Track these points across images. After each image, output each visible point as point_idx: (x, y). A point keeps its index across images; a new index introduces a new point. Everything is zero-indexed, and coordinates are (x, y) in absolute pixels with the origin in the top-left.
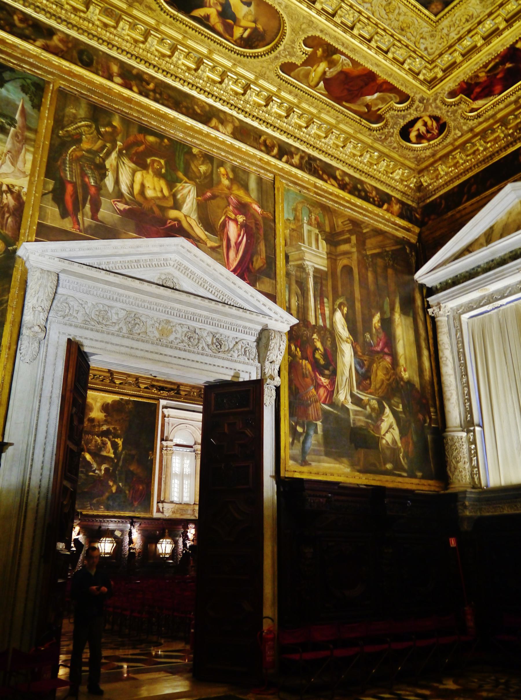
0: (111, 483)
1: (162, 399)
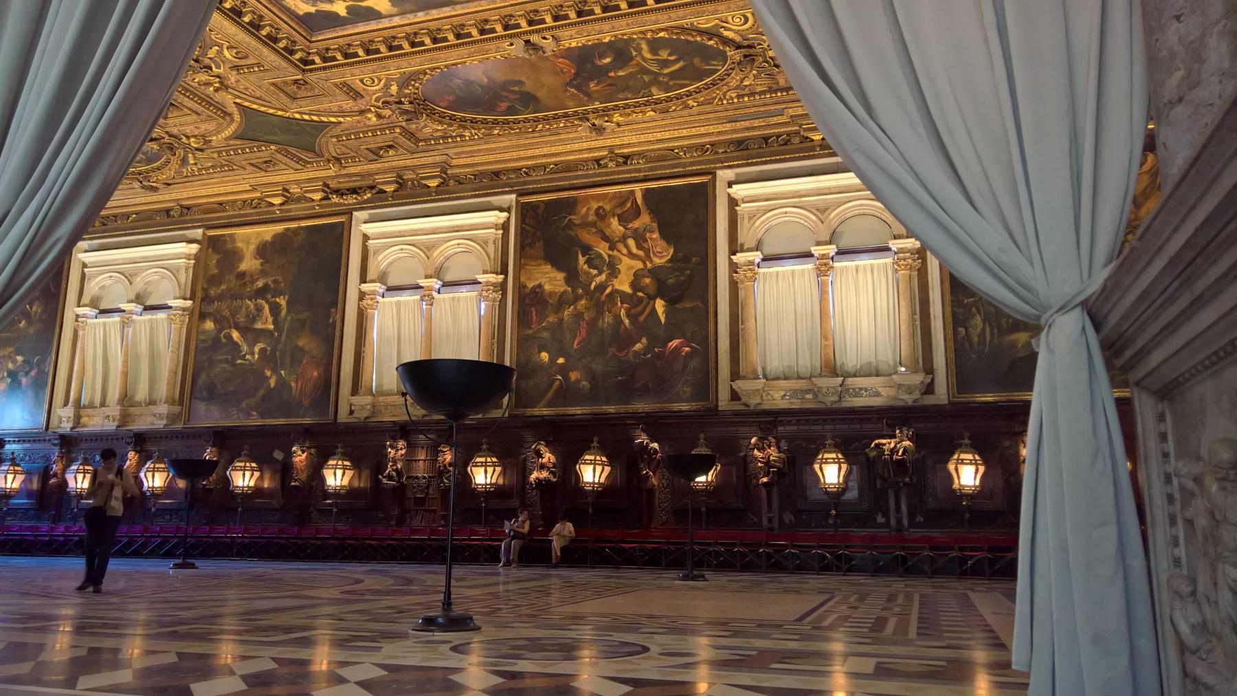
0: (268, 373)
1: (356, 209)
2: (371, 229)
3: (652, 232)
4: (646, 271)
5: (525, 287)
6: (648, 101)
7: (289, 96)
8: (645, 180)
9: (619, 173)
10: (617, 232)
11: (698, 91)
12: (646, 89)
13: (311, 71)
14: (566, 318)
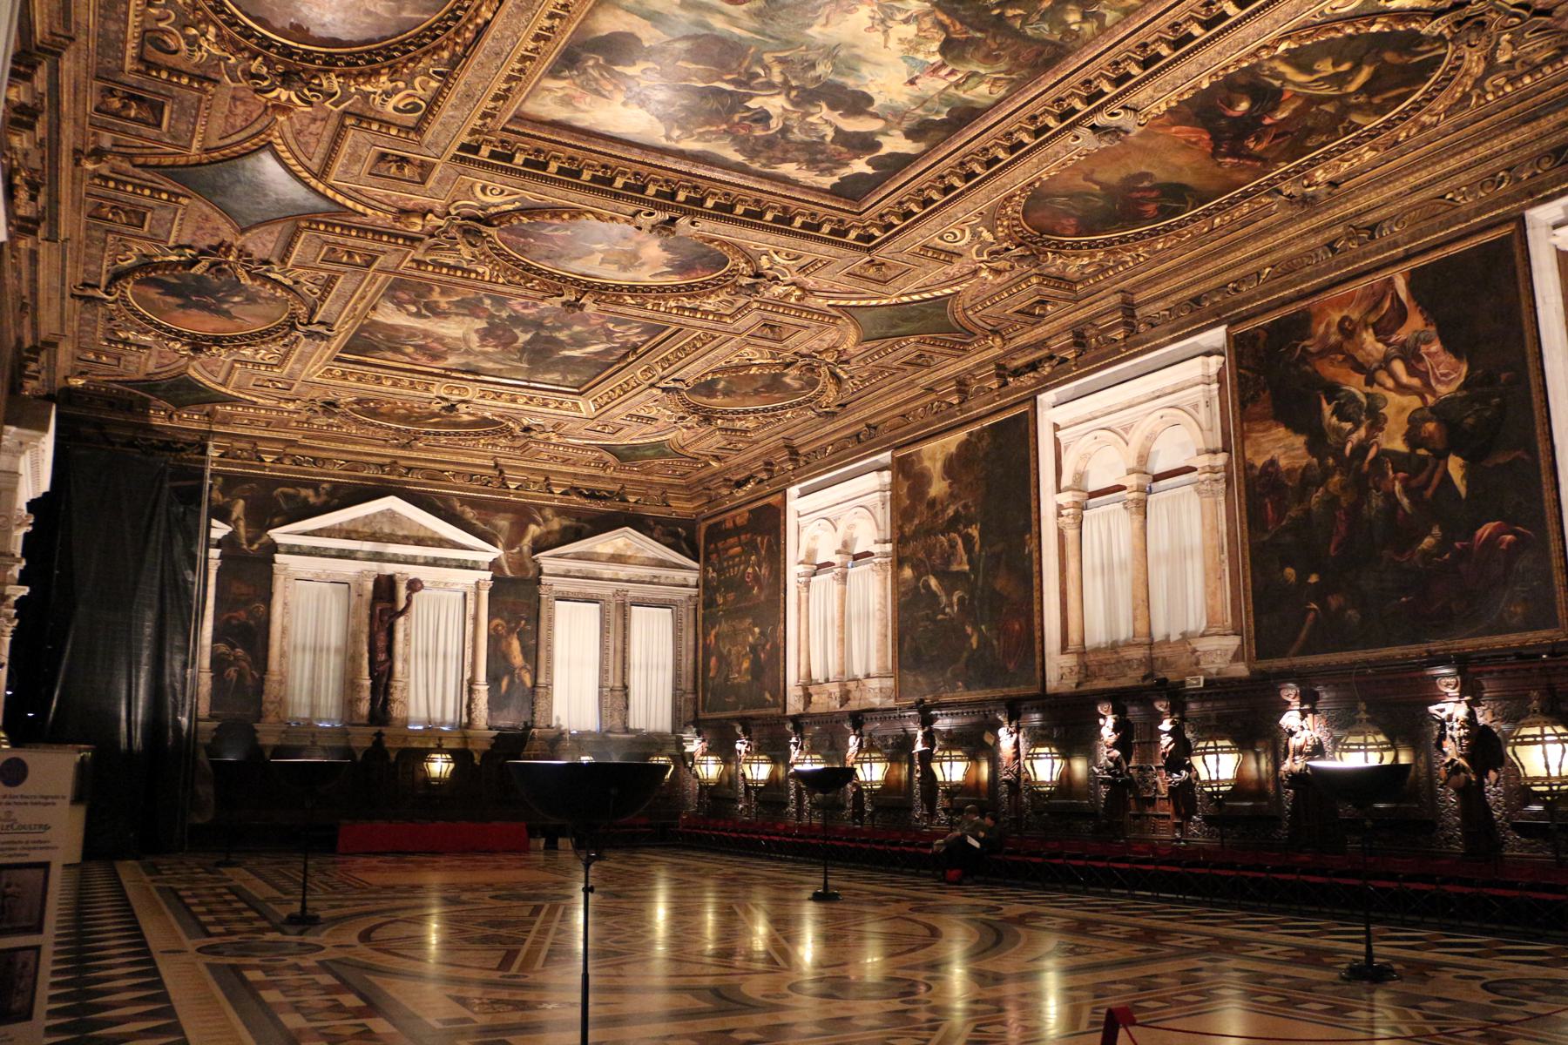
0: (969, 630)
2: (1063, 414)
3: (1428, 342)
4: (1427, 412)
5: (1252, 466)
6: (1358, 137)
7: (877, 281)
8: (1408, 257)
9: (1365, 256)
10: (1375, 354)
11: (1429, 98)
12: (1342, 121)
13: (875, 247)
14: (1314, 509)
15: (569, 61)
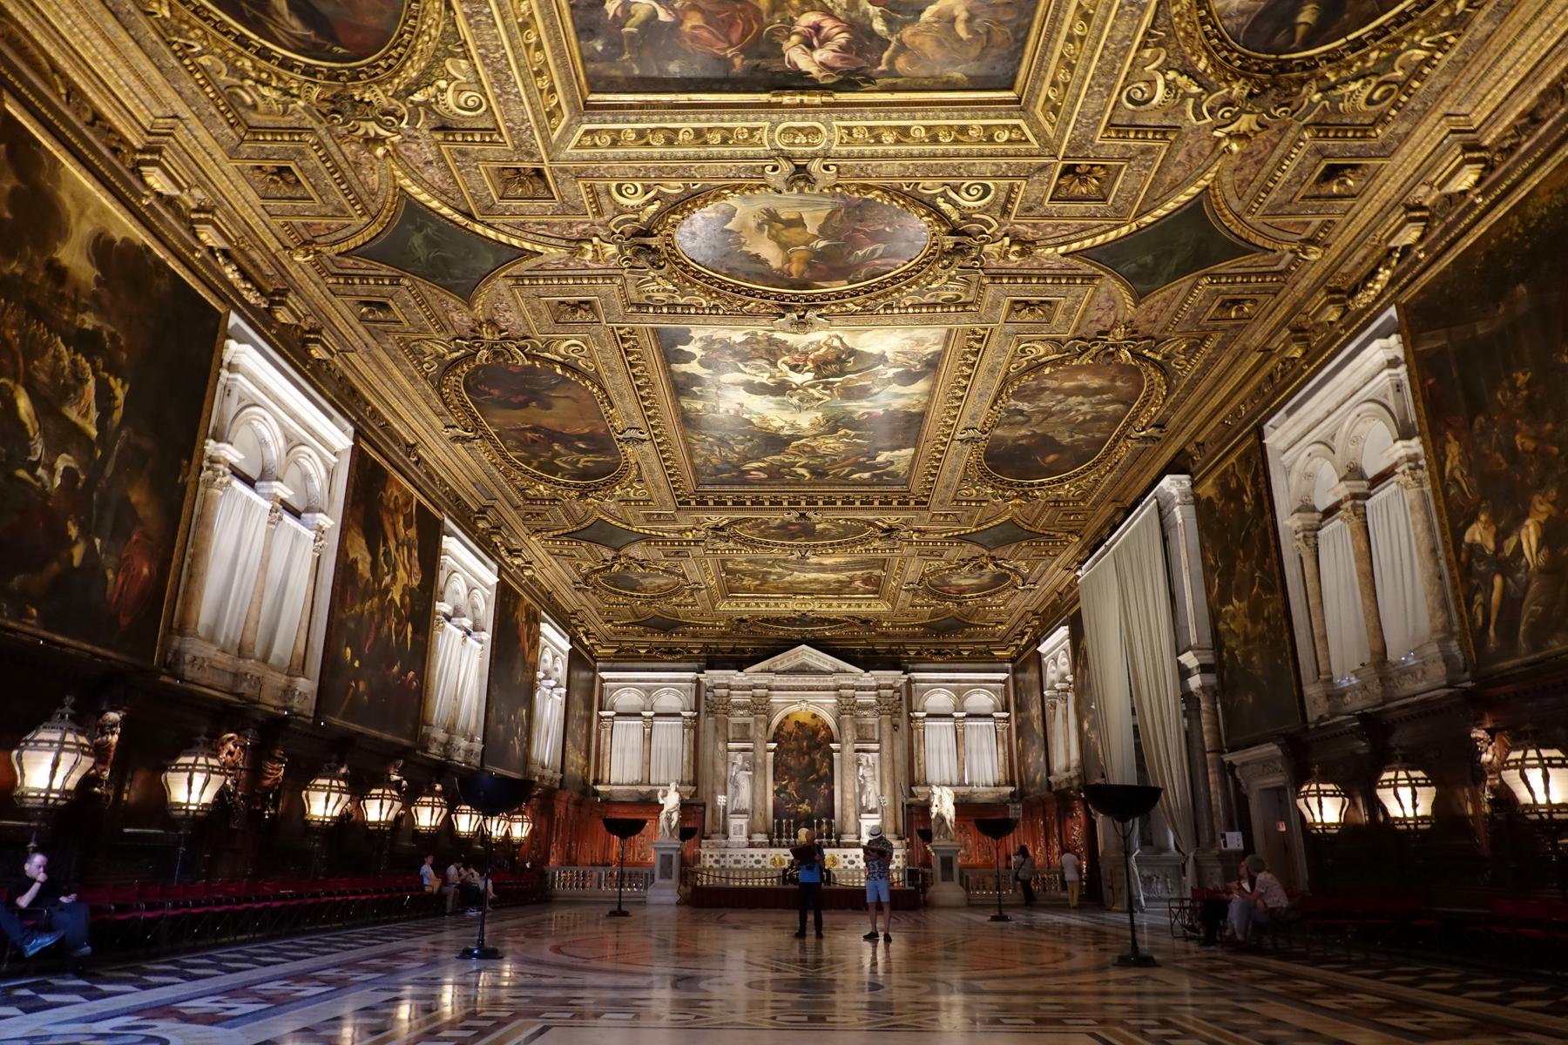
0: (73, 532)
15: (932, 365)
